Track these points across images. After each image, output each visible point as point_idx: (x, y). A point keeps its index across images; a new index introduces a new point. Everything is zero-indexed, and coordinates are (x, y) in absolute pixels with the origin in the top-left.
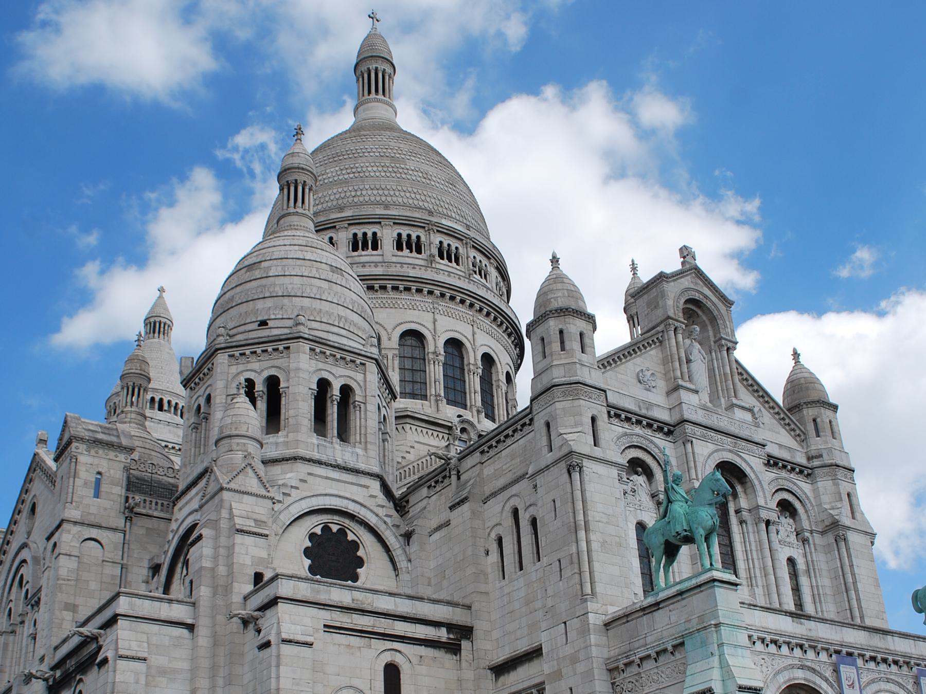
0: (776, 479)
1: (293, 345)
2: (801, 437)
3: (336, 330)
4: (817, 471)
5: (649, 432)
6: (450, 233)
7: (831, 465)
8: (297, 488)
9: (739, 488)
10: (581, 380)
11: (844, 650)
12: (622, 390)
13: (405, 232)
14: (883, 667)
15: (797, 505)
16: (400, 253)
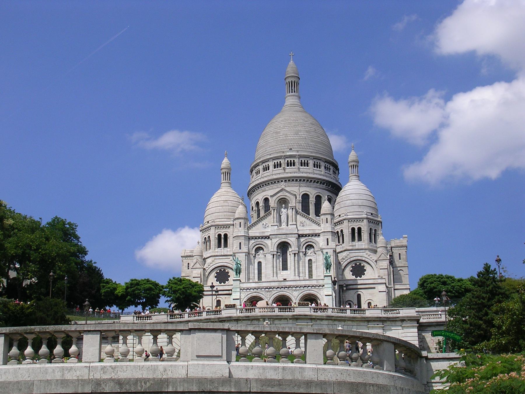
0: (306, 240)
1: (212, 228)
2: (319, 225)
3: (223, 220)
4: (321, 234)
5: (263, 240)
6: (291, 156)
7: (322, 232)
8: (212, 263)
9: (289, 246)
10: (237, 235)
11: (268, 288)
12: (257, 230)
13: (276, 162)
14: (282, 289)
15: (314, 245)
16: (275, 169)
